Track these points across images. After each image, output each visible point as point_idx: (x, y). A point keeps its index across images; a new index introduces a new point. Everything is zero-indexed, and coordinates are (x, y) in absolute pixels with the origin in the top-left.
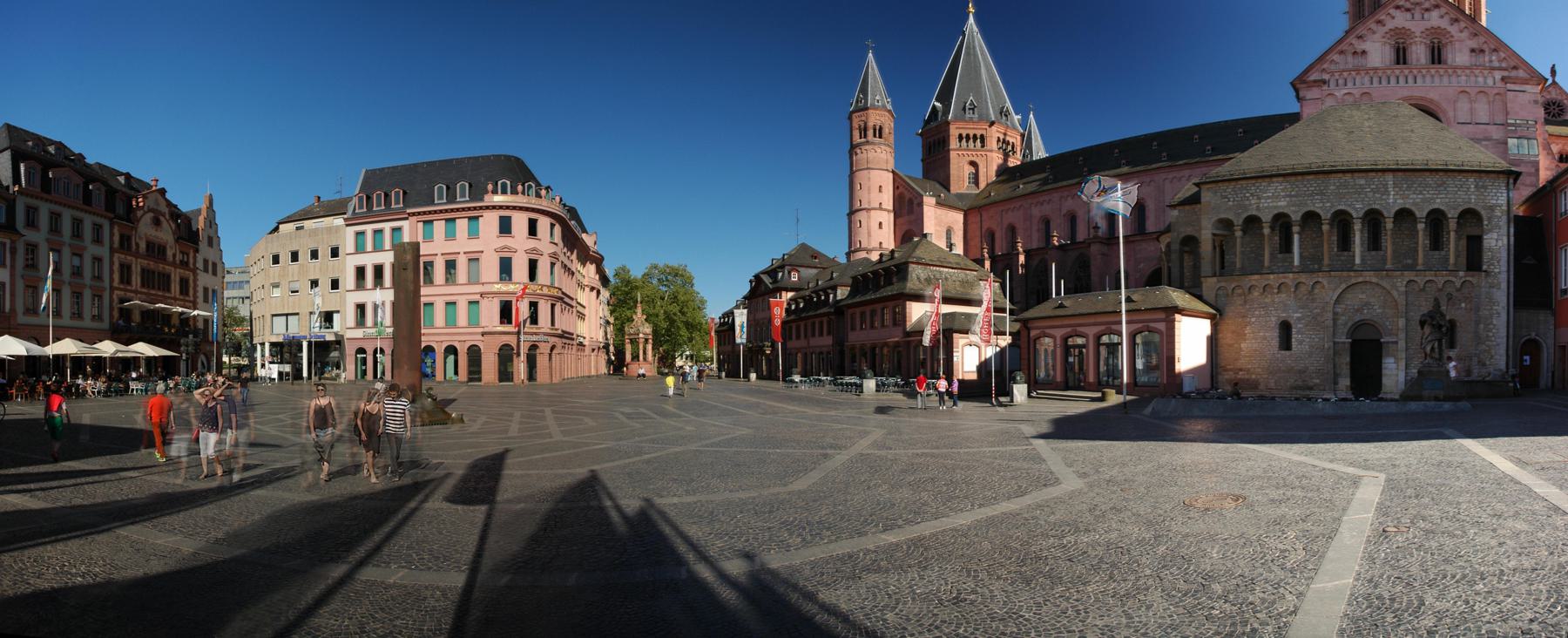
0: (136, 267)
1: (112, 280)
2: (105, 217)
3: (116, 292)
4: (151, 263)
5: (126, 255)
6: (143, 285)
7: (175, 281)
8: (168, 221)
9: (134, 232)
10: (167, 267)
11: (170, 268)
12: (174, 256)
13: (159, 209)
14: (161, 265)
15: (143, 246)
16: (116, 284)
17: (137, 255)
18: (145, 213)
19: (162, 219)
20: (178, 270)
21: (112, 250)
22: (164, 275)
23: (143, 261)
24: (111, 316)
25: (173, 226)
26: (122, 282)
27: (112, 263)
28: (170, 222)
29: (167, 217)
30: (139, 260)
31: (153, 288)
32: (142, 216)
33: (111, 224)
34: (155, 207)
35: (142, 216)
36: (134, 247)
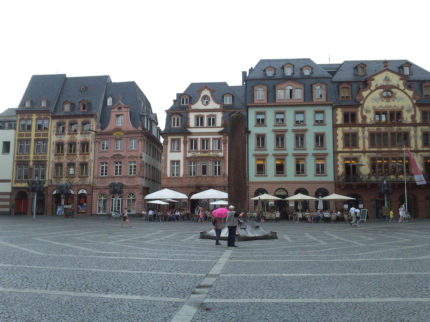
0: (364, 133)
1: (335, 146)
2: (326, 105)
3: (340, 155)
4: (383, 128)
5: (350, 127)
6: (372, 145)
7: (415, 137)
8: (403, 91)
9: (360, 109)
10: (403, 128)
11: (407, 128)
12: (413, 117)
13: (390, 83)
14: (395, 128)
15: (370, 117)
16: (340, 149)
17: (364, 125)
18: (372, 91)
19: (394, 90)
20: (419, 128)
21: (335, 127)
22: (399, 134)
23: (371, 128)
24: (336, 171)
25: (411, 93)
26: (346, 145)
27: (335, 135)
28: (406, 91)
29: (402, 87)
30: (366, 128)
31: (386, 146)
32: (367, 96)
33: (333, 109)
34: (385, 84)
35: (367, 96)
36: (360, 120)
